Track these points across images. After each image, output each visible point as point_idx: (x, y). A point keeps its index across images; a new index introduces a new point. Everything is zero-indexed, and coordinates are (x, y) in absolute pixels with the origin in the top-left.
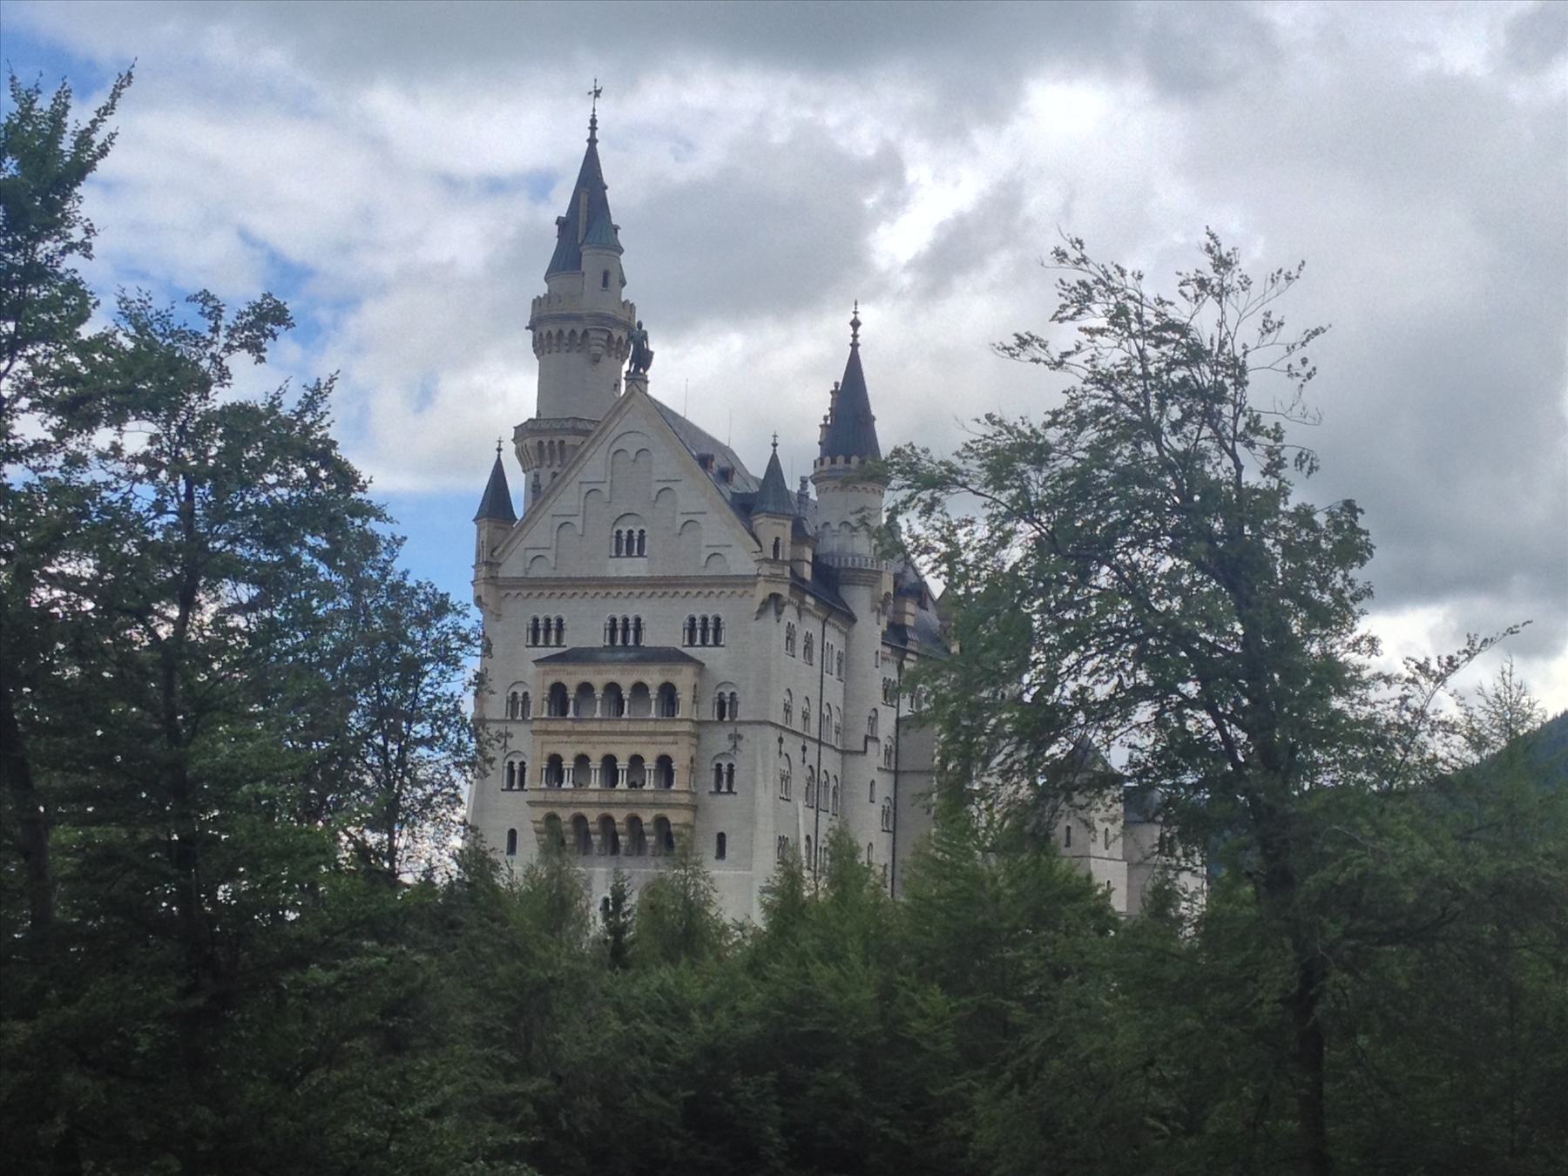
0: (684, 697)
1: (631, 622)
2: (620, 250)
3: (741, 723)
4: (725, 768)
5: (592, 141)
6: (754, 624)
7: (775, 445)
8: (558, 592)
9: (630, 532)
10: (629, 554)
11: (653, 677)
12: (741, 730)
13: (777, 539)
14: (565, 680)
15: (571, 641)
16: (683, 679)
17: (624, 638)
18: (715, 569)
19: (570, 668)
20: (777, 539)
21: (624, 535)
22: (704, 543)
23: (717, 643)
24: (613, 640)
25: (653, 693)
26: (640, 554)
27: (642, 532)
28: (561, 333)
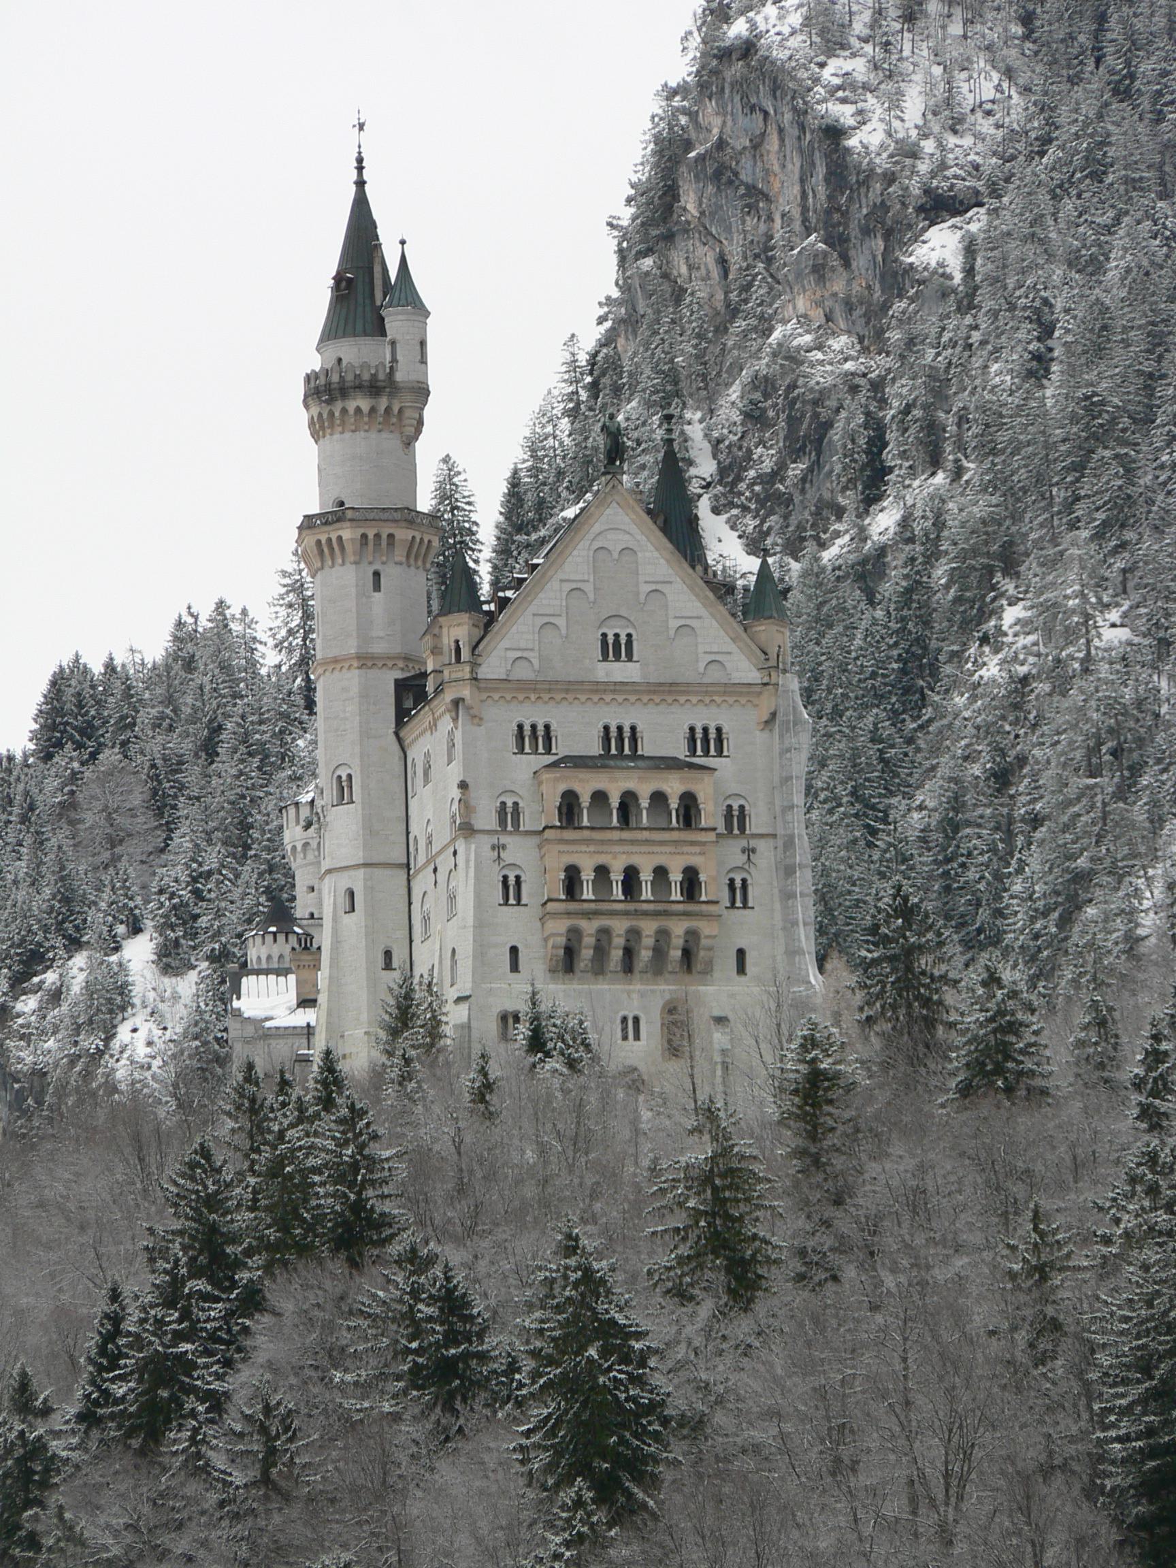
1: (627, 729)
2: (427, 314)
3: (754, 836)
4: (738, 884)
5: (360, 184)
8: (546, 697)
9: (617, 635)
10: (617, 657)
11: (673, 786)
12: (753, 843)
14: (577, 788)
15: (562, 748)
17: (620, 746)
18: (715, 675)
19: (583, 774)
21: (611, 639)
23: (720, 753)
24: (607, 746)
25: (674, 804)
26: (630, 657)
27: (629, 636)
28: (373, 410)
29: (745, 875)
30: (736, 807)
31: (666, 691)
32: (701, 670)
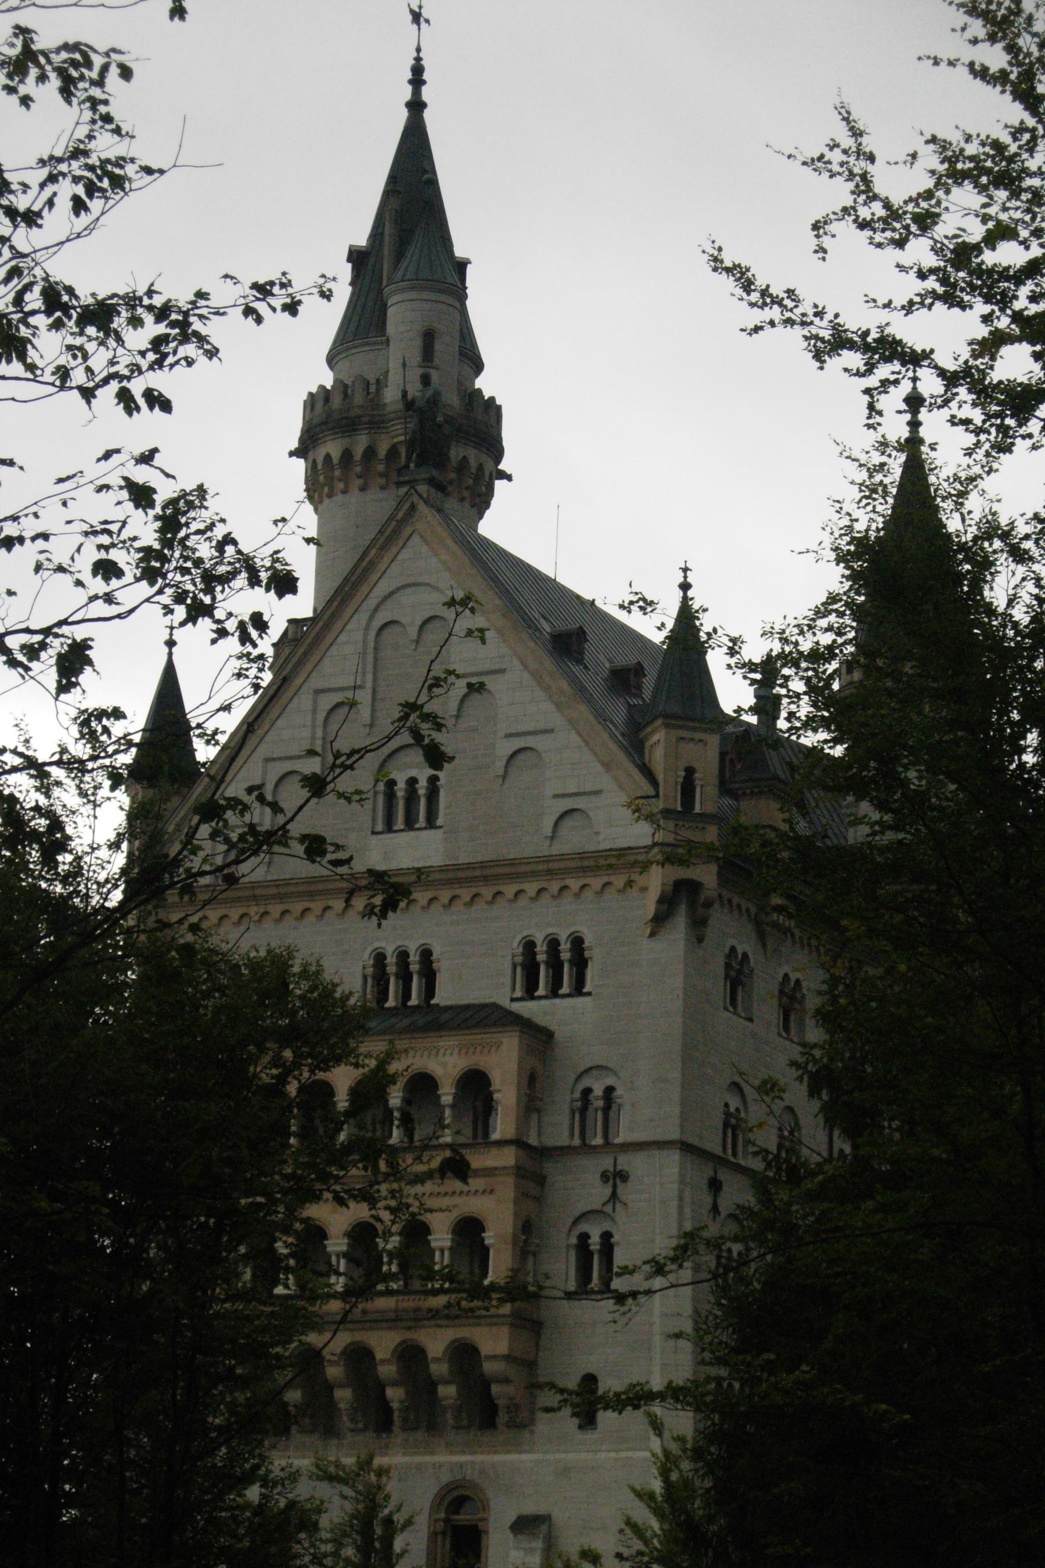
0: (506, 1095)
3: (628, 1147)
4: (595, 1241)
5: (416, 106)
6: (646, 943)
7: (685, 587)
9: (412, 782)
10: (410, 824)
12: (624, 1161)
13: (690, 771)
16: (503, 1062)
18: (574, 840)
20: (690, 771)
21: (401, 787)
22: (552, 788)
23: (578, 989)
25: (447, 1095)
26: (431, 822)
28: (347, 456)
29: (606, 1226)
30: (598, 1091)
31: (476, 880)
32: (548, 830)
